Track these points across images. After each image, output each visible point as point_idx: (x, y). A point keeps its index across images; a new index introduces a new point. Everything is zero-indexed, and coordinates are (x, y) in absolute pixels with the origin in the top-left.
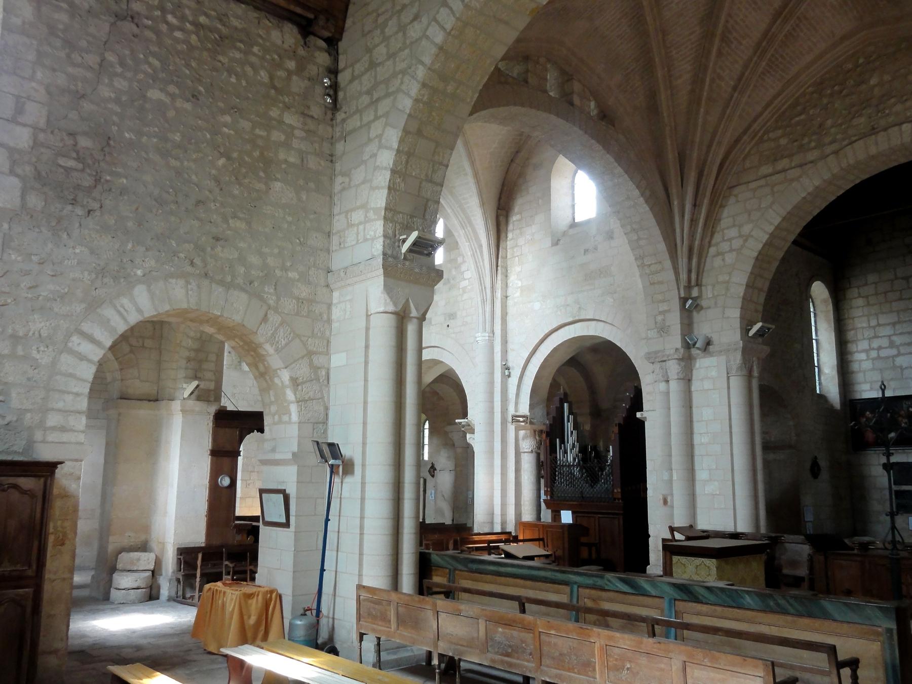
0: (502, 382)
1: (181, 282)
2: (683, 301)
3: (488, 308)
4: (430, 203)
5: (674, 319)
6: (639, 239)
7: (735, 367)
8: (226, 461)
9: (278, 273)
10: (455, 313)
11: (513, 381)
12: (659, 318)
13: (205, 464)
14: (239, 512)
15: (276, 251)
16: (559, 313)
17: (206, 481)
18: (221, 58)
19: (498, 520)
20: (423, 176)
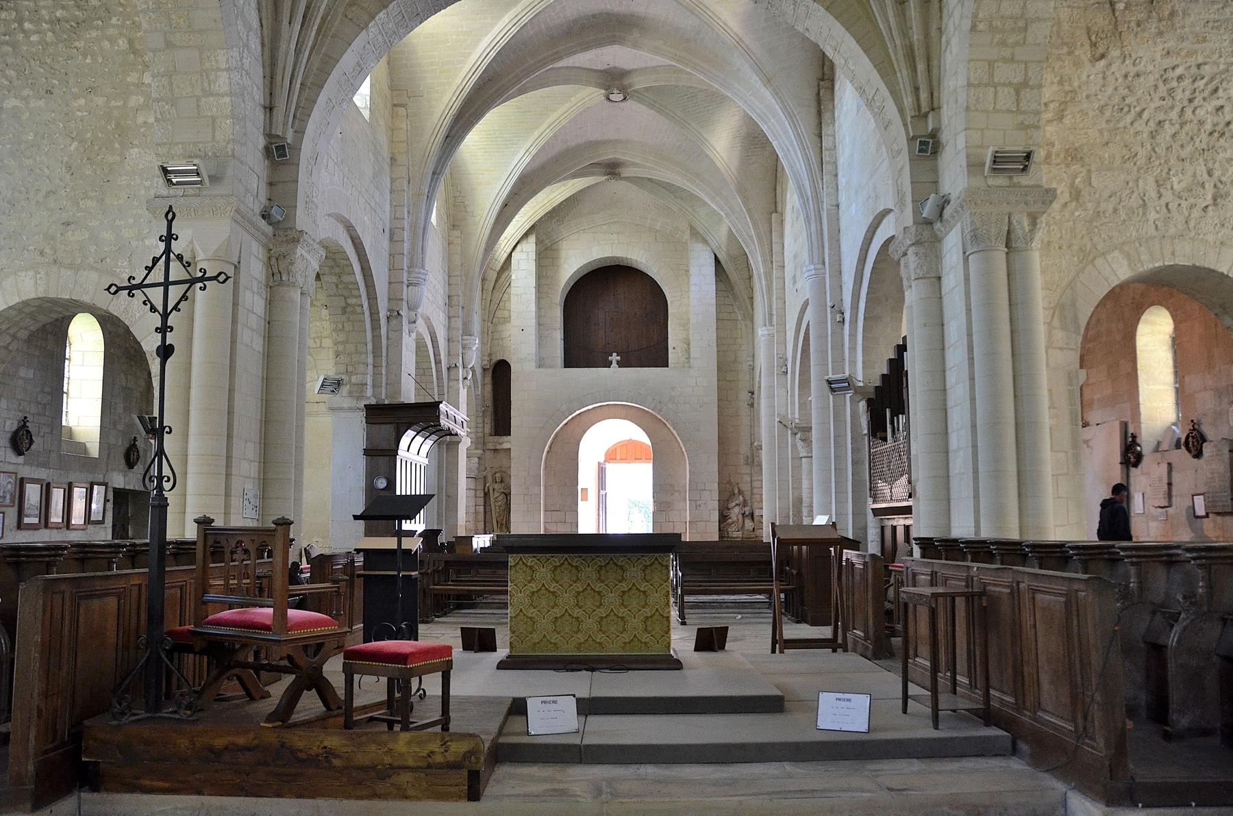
1: (31, 273)
4: (218, 121)
7: (968, 237)
8: (382, 461)
9: (134, 244)
13: (360, 464)
14: (717, 539)
15: (131, 221)
17: (362, 484)
18: (77, 44)
20: (198, 92)
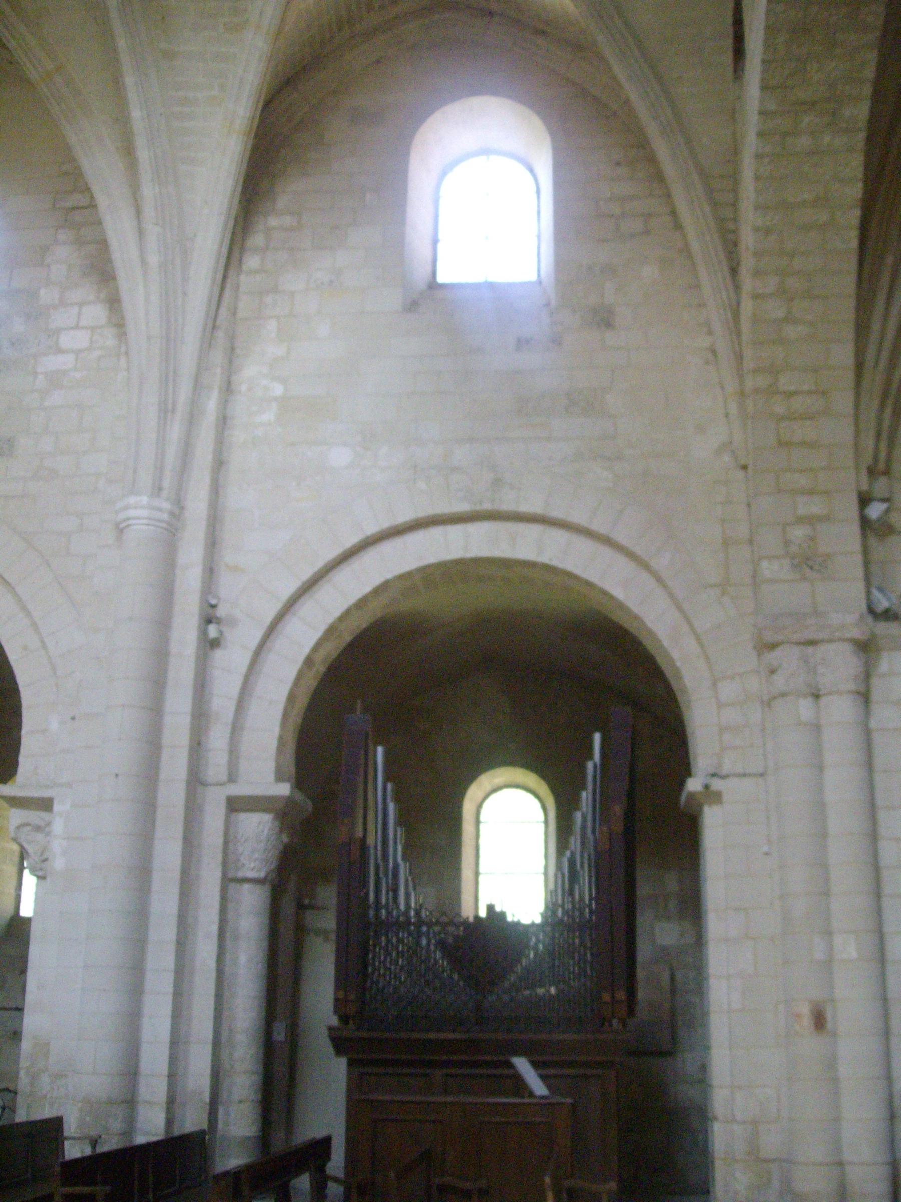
0: (198, 657)
2: (864, 501)
3: (175, 431)
5: (843, 539)
6: (789, 319)
10: (10, 442)
11: (232, 660)
12: (799, 533)
16: (422, 485)
19: (153, 1088)
